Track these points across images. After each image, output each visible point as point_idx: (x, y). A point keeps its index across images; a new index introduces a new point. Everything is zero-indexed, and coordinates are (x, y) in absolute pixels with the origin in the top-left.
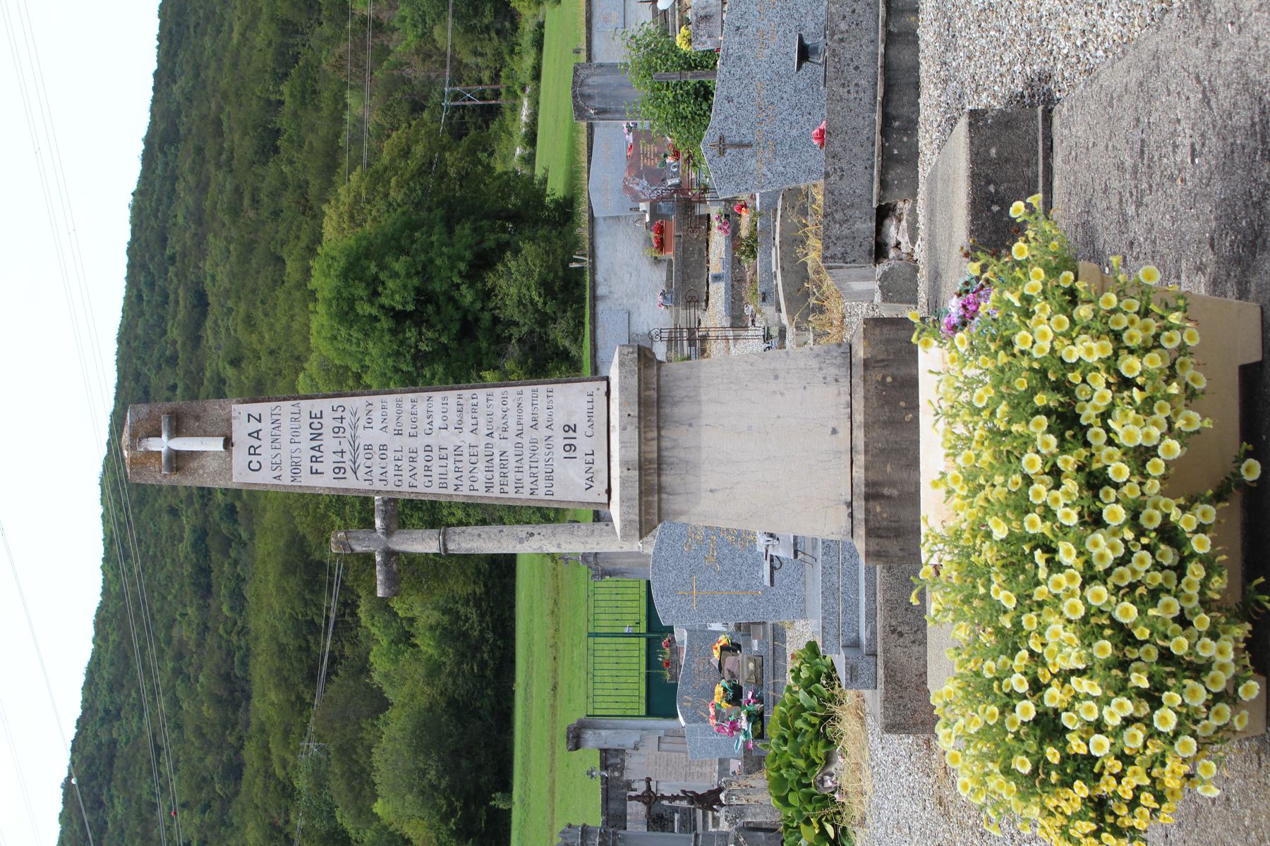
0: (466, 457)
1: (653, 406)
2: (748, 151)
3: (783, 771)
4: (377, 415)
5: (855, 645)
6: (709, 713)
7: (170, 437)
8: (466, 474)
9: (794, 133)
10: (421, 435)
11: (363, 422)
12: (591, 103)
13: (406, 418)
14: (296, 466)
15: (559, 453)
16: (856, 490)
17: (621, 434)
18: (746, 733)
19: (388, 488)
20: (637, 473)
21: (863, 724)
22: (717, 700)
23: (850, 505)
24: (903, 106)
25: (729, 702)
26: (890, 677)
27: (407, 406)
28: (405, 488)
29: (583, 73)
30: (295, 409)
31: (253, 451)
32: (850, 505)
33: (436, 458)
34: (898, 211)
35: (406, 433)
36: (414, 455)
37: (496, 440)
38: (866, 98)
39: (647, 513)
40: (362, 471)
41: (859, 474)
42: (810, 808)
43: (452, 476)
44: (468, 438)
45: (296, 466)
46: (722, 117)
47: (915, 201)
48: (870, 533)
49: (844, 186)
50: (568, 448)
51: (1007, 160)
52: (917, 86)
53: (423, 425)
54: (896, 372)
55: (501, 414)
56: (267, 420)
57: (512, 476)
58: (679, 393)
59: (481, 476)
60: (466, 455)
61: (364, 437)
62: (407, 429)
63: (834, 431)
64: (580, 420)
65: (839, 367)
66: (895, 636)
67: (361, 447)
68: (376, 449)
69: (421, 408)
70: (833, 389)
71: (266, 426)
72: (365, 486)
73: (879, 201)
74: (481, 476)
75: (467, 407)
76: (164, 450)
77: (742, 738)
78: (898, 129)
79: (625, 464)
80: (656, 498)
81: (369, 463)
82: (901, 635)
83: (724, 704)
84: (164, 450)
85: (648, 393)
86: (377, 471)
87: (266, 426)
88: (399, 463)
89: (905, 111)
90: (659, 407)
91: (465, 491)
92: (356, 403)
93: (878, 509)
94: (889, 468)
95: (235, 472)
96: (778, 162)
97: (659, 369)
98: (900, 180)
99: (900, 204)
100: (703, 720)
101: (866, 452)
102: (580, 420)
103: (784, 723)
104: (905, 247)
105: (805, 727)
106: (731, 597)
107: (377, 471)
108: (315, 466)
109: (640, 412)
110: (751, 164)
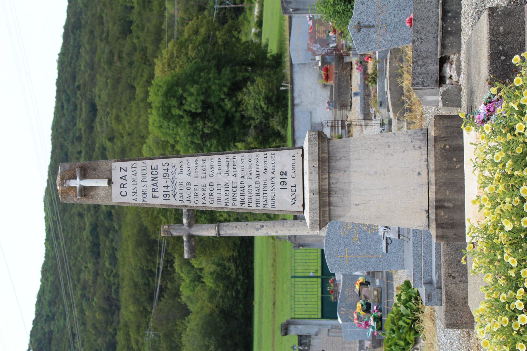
0: (230, 188)
1: (326, 162)
2: (372, 30)
3: (393, 347)
4: (185, 167)
5: (430, 283)
6: (353, 317)
7: (81, 179)
8: (231, 197)
9: (396, 20)
10: (208, 177)
11: (178, 171)
12: (290, 5)
13: (200, 169)
14: (144, 193)
15: (278, 186)
16: (431, 204)
17: (309, 176)
18: (373, 328)
20: (318, 196)
21: (434, 324)
22: (358, 310)
23: (428, 211)
24: (453, 5)
25: (364, 311)
26: (449, 299)
27: (200, 163)
28: (200, 204)
31: (123, 186)
32: (428, 211)
34: (451, 60)
35: (200, 176)
37: (246, 180)
39: (323, 216)
40: (178, 196)
41: (432, 195)
43: (223, 198)
44: (231, 179)
45: (144, 193)
46: (359, 12)
47: (460, 54)
48: (438, 226)
49: (423, 47)
51: (509, 33)
53: (209, 172)
54: (451, 143)
55: (248, 166)
56: (129, 170)
57: (254, 198)
58: (339, 155)
59: (238, 198)
61: (179, 179)
62: (200, 174)
63: (419, 174)
64: (288, 169)
65: (421, 140)
66: (451, 278)
67: (177, 184)
68: (185, 184)
69: (208, 164)
70: (418, 152)
71: (129, 173)
72: (179, 203)
73: (441, 54)
74: (238, 198)
76: (78, 186)
77: (371, 330)
78: (451, 17)
79: (312, 192)
80: (328, 209)
81: (181, 192)
82: (454, 278)
83: (362, 313)
84: (78, 186)
85: (323, 155)
86: (185, 196)
87: (129, 173)
88: (197, 192)
89: (454, 8)
90: (329, 162)
91: (230, 205)
92: (175, 161)
93: (442, 214)
94: (448, 193)
95: (114, 197)
96: (388, 35)
97: (328, 143)
98: (452, 44)
99: (452, 56)
100: (351, 321)
101: (436, 184)
102: (288, 169)
103: (393, 323)
104: (455, 78)
105: (404, 324)
106: (365, 258)
107: (185, 196)
108: (154, 193)
109: (319, 165)
110: (374, 36)
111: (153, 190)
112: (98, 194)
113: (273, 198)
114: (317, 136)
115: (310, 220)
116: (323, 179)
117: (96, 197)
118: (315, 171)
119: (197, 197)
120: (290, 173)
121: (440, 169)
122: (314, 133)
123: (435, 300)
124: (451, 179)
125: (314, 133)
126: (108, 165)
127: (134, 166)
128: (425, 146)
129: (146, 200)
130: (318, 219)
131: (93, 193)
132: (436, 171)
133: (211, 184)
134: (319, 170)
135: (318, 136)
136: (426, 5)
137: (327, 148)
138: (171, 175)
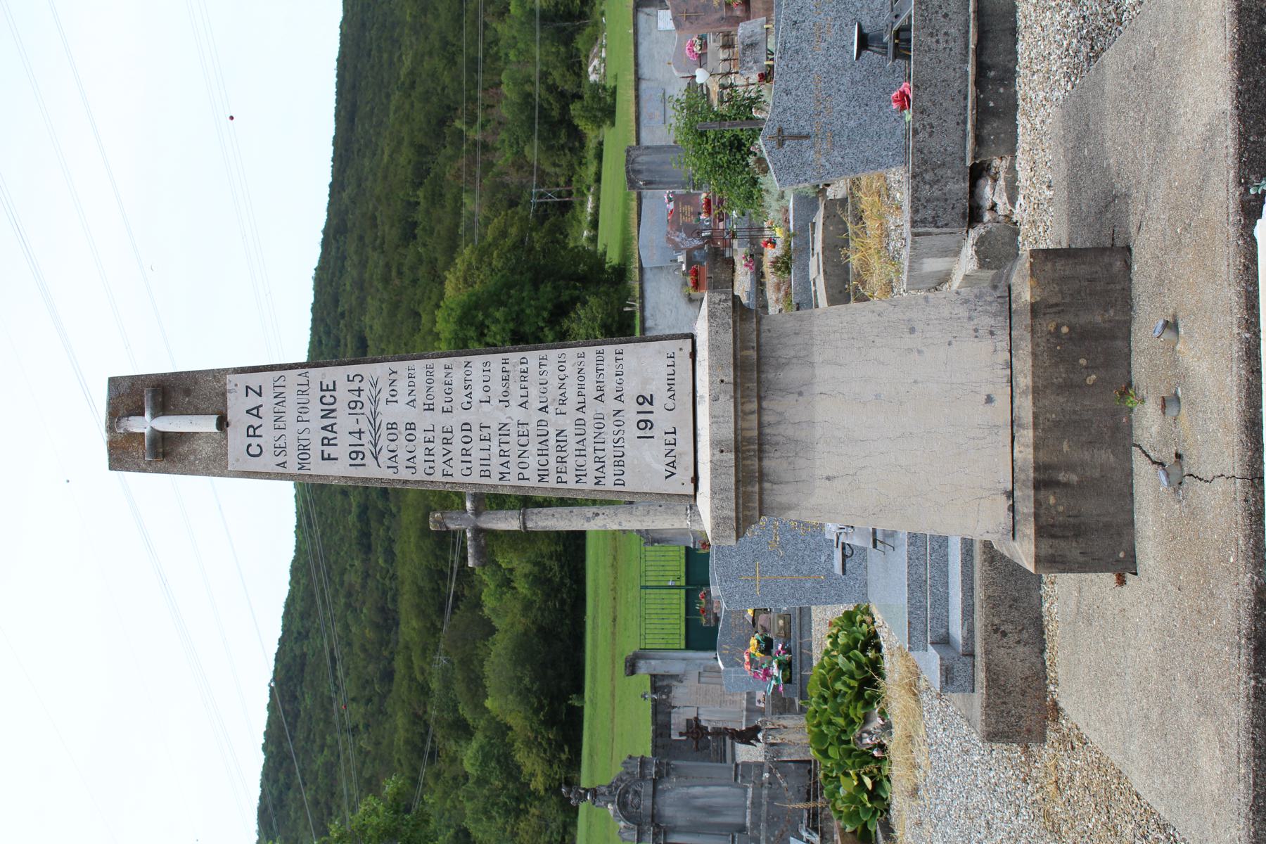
0: (513, 438)
1: (753, 368)
2: (806, 142)
3: (824, 728)
4: (402, 386)
5: (944, 642)
6: (743, 660)
7: (154, 416)
8: (514, 459)
9: (852, 124)
10: (458, 410)
11: (385, 395)
12: (640, 176)
13: (438, 389)
14: (304, 450)
15: (631, 431)
16: (1020, 476)
18: (777, 679)
19: (417, 477)
20: (732, 456)
21: (917, 701)
22: (752, 650)
23: (1010, 495)
24: (999, 54)
25: (762, 652)
26: (993, 680)
27: (439, 374)
28: (438, 477)
29: (634, 153)
30: (303, 380)
31: (252, 431)
33: (476, 438)
34: (993, 171)
35: (438, 408)
36: (448, 436)
37: (551, 416)
38: (957, 47)
39: (746, 508)
40: (384, 456)
41: (1025, 454)
42: (849, 762)
44: (516, 413)
45: (304, 450)
46: (780, 109)
47: (1014, 157)
48: (1042, 532)
49: (934, 144)
50: (642, 425)
52: (1014, 32)
53: (459, 397)
55: (557, 383)
56: (268, 393)
57: (572, 462)
58: (786, 353)
59: (533, 461)
60: (514, 436)
61: (387, 413)
62: (439, 403)
63: (989, 399)
64: (658, 388)
65: (995, 315)
66: (998, 636)
67: (384, 426)
68: (402, 428)
69: (458, 376)
70: (986, 345)
72: (388, 474)
73: (975, 158)
74: (533, 461)
75: (515, 375)
76: (147, 431)
77: (774, 682)
79: (716, 444)
80: (756, 488)
81: (393, 446)
82: (1004, 634)
83: (758, 654)
84: (147, 431)
85: (745, 353)
86: (403, 456)
87: (268, 401)
88: (430, 446)
89: (1001, 59)
90: (759, 371)
91: (513, 480)
92: (377, 371)
93: (1052, 500)
94: (1065, 447)
96: (836, 153)
97: (759, 322)
98: (997, 135)
99: (996, 162)
100: (739, 665)
101: (1035, 426)
102: (658, 388)
104: (1003, 208)
105: (844, 689)
106: (793, 581)
107: (403, 456)
108: (328, 450)
109: (735, 378)
110: (810, 155)
111: (326, 441)
112: (195, 450)
113: (619, 462)
114: (730, 304)
115: (713, 518)
116: (745, 413)
118: (725, 392)
119: (431, 458)
120: (661, 398)
121: (1046, 387)
122: (723, 297)
123: (961, 680)
124: (1075, 412)
125: (723, 297)
126: (219, 381)
127: (280, 383)
129: (307, 466)
130: (733, 514)
131: (184, 449)
132: (1037, 392)
133: (466, 427)
134: (735, 391)
135: (734, 303)
136: (941, 56)
137: (754, 336)
138: (368, 405)
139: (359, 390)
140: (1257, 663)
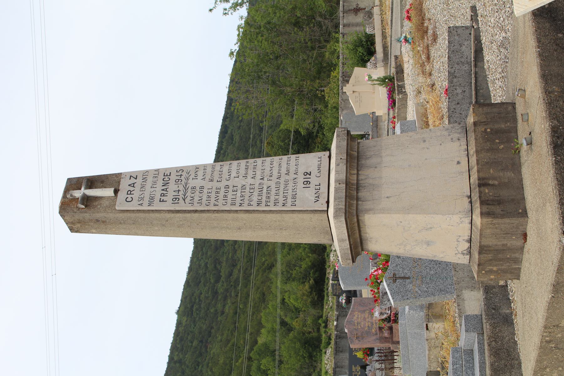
0: (248, 189)
2: (408, 281)
7: (86, 188)
8: (247, 198)
9: (432, 272)
11: (193, 176)
15: (300, 185)
20: (344, 185)
32: (470, 197)
35: (215, 180)
36: (218, 190)
45: (152, 198)
50: (306, 183)
54: (492, 127)
61: (192, 183)
62: (216, 178)
63: (458, 163)
64: (314, 170)
65: (460, 133)
67: (190, 188)
68: (198, 188)
70: (457, 144)
81: (193, 195)
86: (196, 199)
90: (358, 161)
93: (487, 191)
94: (491, 171)
96: (424, 286)
101: (478, 164)
102: (314, 170)
107: (196, 199)
108: (162, 198)
110: (410, 287)
113: (294, 197)
117: (99, 207)
120: (315, 172)
121: (481, 150)
124: (495, 159)
128: (464, 137)
130: (344, 207)
134: (347, 163)
138: (184, 180)
139: (181, 175)
140: (555, 152)
